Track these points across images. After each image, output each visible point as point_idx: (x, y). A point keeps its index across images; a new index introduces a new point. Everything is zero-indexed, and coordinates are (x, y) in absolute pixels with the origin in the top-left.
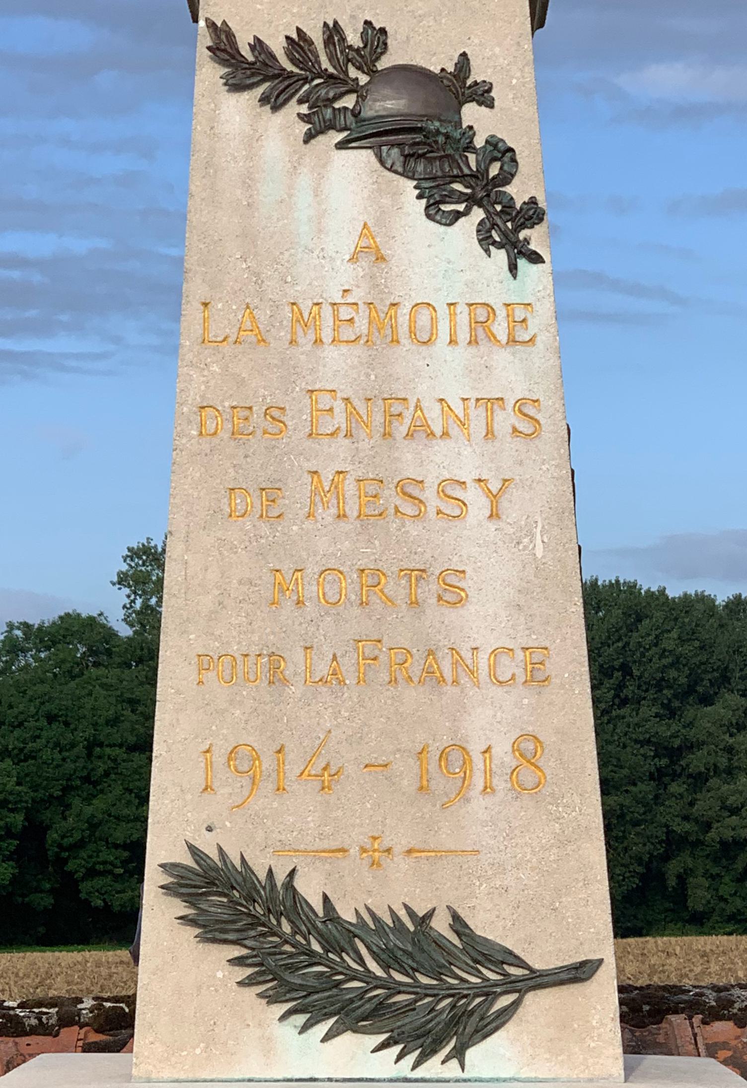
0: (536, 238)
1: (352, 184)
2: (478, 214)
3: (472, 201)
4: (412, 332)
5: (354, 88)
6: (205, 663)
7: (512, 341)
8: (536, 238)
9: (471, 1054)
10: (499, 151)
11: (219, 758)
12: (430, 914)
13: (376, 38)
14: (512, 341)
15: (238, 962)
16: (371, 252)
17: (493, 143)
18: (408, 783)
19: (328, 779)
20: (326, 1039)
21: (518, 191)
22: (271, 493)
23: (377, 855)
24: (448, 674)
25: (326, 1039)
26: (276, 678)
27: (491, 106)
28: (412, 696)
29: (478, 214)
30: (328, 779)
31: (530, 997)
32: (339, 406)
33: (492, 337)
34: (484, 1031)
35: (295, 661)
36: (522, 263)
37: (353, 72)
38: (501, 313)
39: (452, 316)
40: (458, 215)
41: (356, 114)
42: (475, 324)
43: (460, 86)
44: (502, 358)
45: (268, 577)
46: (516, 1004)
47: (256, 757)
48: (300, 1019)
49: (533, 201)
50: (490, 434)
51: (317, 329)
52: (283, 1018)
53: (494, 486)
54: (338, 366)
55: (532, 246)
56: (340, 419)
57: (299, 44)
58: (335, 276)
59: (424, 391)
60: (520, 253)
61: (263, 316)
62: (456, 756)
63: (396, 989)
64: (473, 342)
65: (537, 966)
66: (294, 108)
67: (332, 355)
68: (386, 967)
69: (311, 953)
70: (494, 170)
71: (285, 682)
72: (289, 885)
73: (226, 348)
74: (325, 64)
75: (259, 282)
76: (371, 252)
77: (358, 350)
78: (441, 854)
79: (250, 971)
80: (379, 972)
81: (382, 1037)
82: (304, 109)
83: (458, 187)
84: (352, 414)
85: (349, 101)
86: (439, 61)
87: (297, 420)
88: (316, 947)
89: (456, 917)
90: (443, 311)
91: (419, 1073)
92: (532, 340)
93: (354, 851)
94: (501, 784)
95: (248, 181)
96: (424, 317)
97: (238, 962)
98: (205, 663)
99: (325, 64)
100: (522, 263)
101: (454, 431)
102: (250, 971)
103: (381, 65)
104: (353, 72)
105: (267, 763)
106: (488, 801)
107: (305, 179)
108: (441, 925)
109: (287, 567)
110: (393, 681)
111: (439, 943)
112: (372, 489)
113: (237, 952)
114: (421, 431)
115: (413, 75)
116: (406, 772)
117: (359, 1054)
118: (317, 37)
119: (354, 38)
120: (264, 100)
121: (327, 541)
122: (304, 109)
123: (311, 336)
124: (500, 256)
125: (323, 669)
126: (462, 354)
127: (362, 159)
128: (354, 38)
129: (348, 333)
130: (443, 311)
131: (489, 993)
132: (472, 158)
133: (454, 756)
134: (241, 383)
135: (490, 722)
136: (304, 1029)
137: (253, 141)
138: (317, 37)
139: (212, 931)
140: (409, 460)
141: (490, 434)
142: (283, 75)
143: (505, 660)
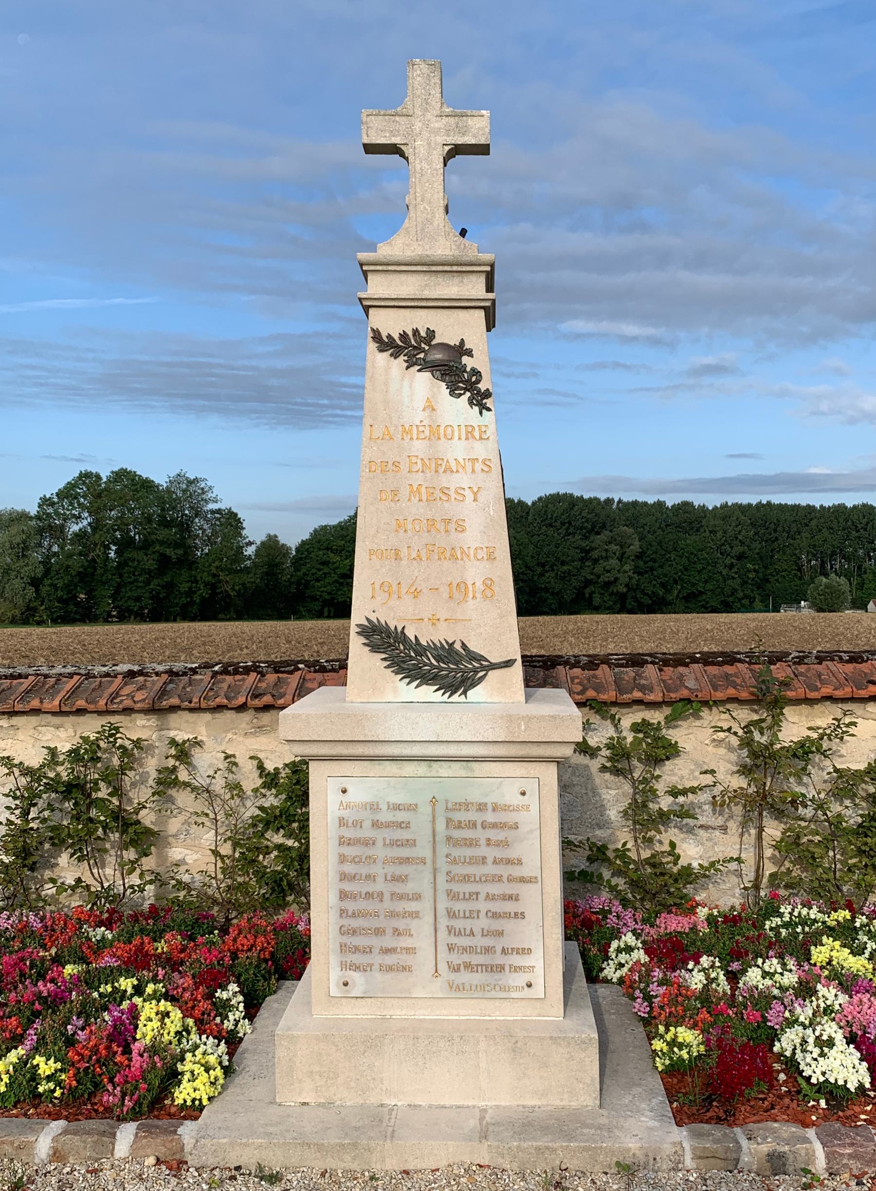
0: (489, 402)
1: (424, 383)
2: (468, 394)
3: (466, 389)
4: (445, 435)
5: (424, 351)
6: (371, 552)
7: (481, 438)
8: (489, 402)
9: (469, 693)
10: (475, 372)
11: (377, 587)
12: (454, 643)
13: (431, 334)
14: (481, 438)
15: (384, 659)
16: (430, 407)
17: (473, 369)
18: (445, 595)
19: (416, 594)
20: (417, 687)
21: (482, 386)
22: (395, 492)
23: (434, 621)
24: (459, 557)
25: (417, 687)
26: (398, 558)
27: (472, 356)
28: (446, 564)
29: (468, 394)
30: (416, 594)
31: (490, 672)
32: (419, 462)
33: (474, 437)
34: (473, 685)
35: (404, 552)
36: (484, 411)
37: (423, 345)
38: (477, 429)
39: (459, 430)
40: (461, 395)
41: (424, 360)
42: (467, 432)
43: (461, 350)
44: (478, 445)
45: (394, 522)
46: (485, 675)
47: (390, 586)
48: (407, 680)
49: (488, 390)
50: (473, 471)
51: (412, 434)
52: (401, 680)
53: (475, 490)
54: (419, 447)
55: (488, 405)
56: (419, 465)
57: (404, 336)
58: (416, 415)
59: (450, 456)
60: (483, 408)
61: (392, 429)
62: (462, 585)
63: (442, 669)
64: (467, 439)
65: (493, 661)
66: (402, 358)
67: (417, 443)
68: (438, 662)
69: (411, 656)
70: (474, 379)
71: (401, 559)
72: (403, 632)
73: (379, 441)
74: (413, 342)
75: (390, 418)
76: (430, 407)
77: (426, 441)
78: (457, 621)
79: (388, 663)
80: (436, 664)
81: (437, 687)
82: (406, 358)
83: (461, 385)
84: (424, 464)
85: (422, 355)
86: (454, 341)
87: (404, 466)
88: (413, 654)
89: (463, 643)
90: (456, 428)
91: (451, 700)
92: (488, 438)
93: (426, 620)
94: (478, 595)
95: (386, 383)
96: (449, 430)
97: (384, 659)
98: (371, 552)
99: (413, 342)
100: (484, 411)
101: (460, 470)
102: (388, 663)
103: (433, 343)
104: (423, 345)
105: (395, 588)
106: (474, 602)
107: (406, 383)
108: (458, 646)
109: (401, 518)
110: (440, 559)
111: (457, 653)
112: (431, 491)
113: (384, 656)
114: (448, 470)
115: (444, 346)
116: (444, 592)
117: (428, 693)
118: (410, 334)
119: (423, 334)
120: (391, 355)
121: (415, 510)
122: (406, 358)
123: (409, 437)
124: (476, 409)
125: (414, 555)
126: (463, 442)
127: (427, 375)
128: (423, 334)
129: (422, 436)
130: (456, 428)
131: (476, 672)
132: (466, 375)
133: (462, 586)
134: (384, 453)
135: (475, 573)
136: (408, 684)
137: (388, 369)
138: (410, 334)
139: (375, 648)
140: (445, 480)
141: (473, 471)
142: (398, 346)
143: (479, 551)
